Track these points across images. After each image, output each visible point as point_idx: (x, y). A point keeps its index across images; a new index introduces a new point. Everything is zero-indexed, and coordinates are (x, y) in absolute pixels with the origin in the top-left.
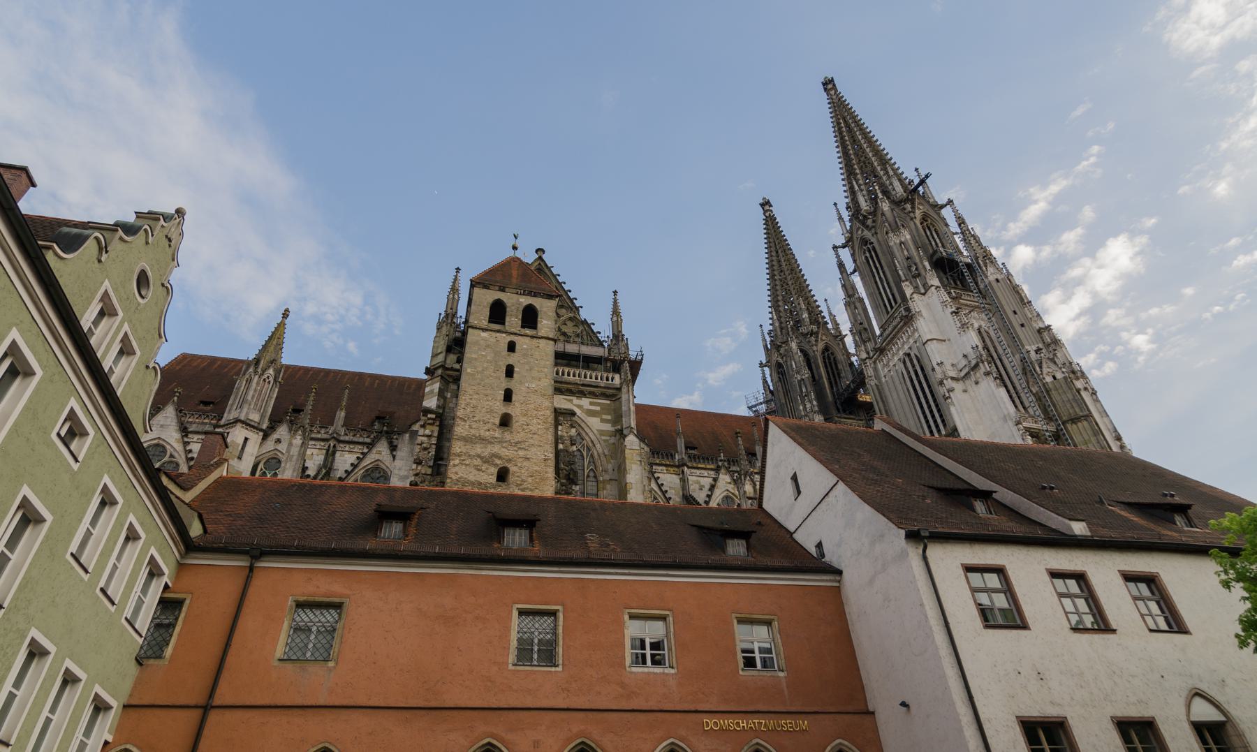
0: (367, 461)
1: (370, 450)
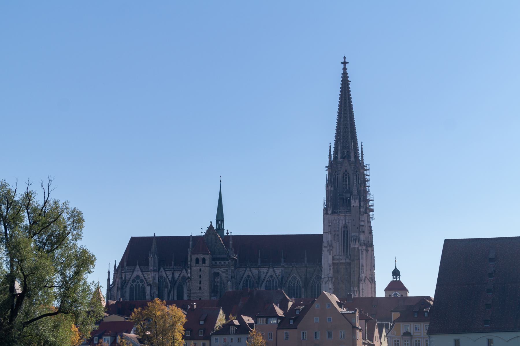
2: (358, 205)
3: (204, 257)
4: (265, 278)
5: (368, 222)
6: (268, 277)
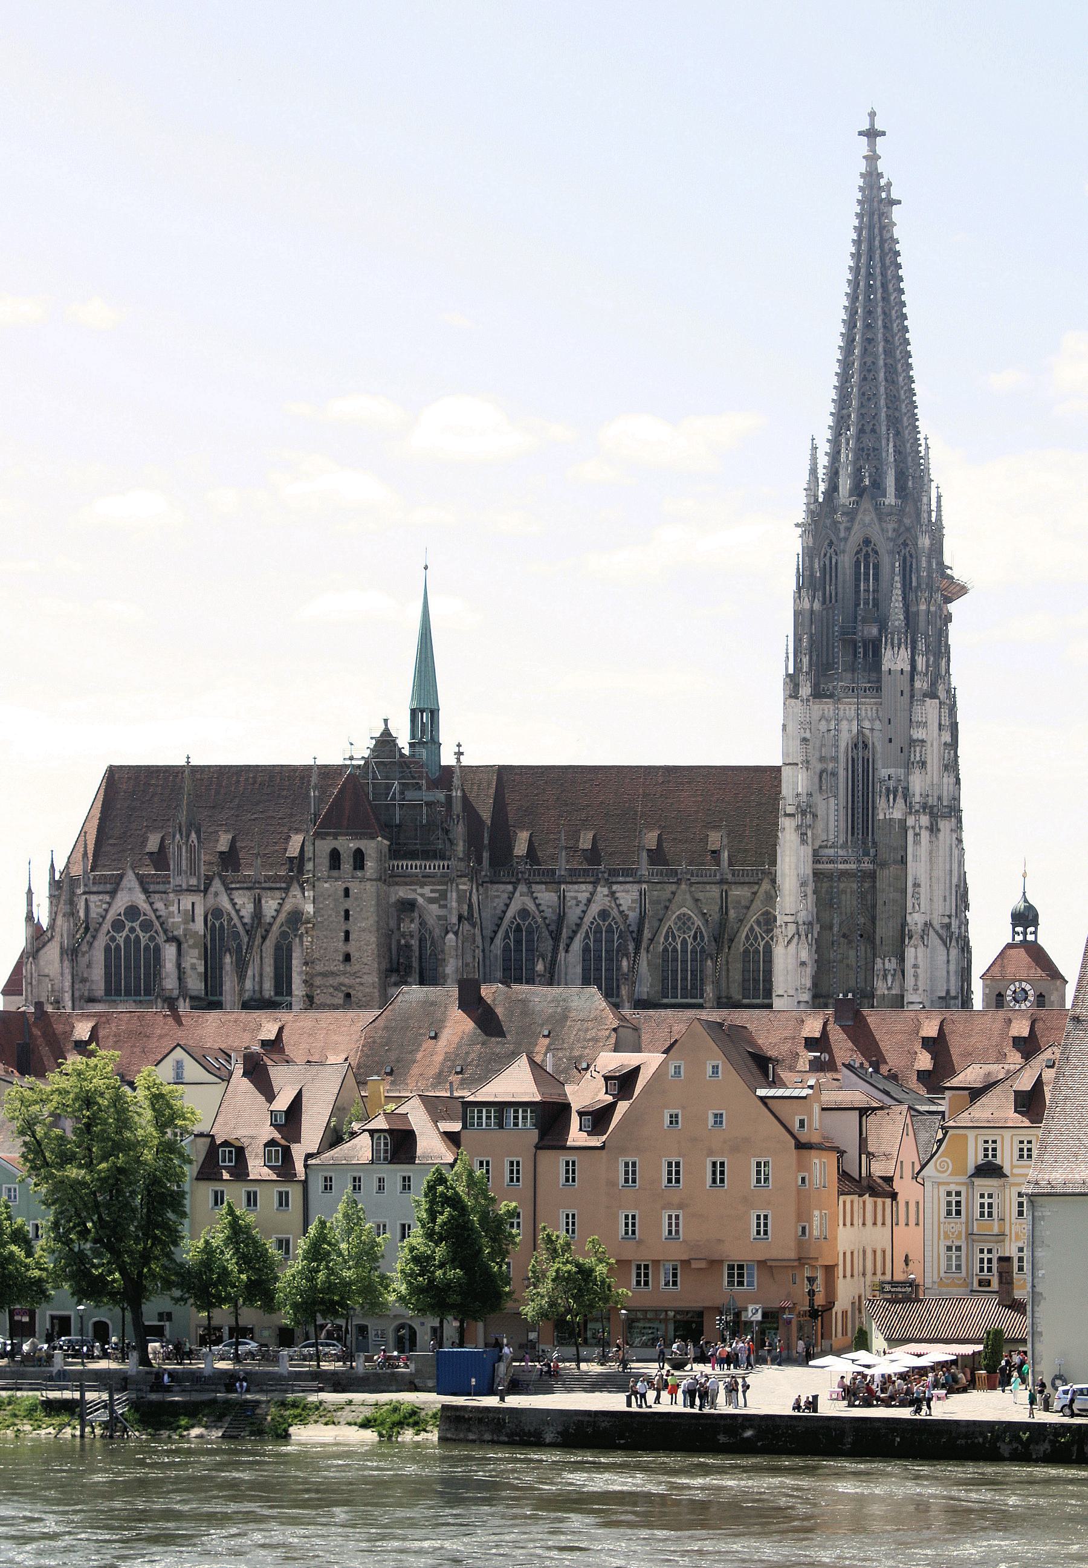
0: (287, 907)
1: (287, 894)
2: (907, 668)
3: (357, 846)
4: (581, 919)
5: (940, 729)
6: (594, 918)
